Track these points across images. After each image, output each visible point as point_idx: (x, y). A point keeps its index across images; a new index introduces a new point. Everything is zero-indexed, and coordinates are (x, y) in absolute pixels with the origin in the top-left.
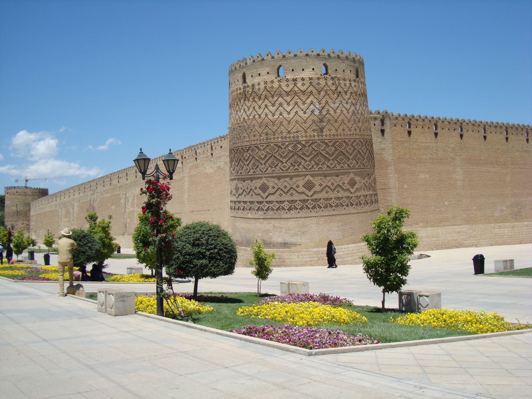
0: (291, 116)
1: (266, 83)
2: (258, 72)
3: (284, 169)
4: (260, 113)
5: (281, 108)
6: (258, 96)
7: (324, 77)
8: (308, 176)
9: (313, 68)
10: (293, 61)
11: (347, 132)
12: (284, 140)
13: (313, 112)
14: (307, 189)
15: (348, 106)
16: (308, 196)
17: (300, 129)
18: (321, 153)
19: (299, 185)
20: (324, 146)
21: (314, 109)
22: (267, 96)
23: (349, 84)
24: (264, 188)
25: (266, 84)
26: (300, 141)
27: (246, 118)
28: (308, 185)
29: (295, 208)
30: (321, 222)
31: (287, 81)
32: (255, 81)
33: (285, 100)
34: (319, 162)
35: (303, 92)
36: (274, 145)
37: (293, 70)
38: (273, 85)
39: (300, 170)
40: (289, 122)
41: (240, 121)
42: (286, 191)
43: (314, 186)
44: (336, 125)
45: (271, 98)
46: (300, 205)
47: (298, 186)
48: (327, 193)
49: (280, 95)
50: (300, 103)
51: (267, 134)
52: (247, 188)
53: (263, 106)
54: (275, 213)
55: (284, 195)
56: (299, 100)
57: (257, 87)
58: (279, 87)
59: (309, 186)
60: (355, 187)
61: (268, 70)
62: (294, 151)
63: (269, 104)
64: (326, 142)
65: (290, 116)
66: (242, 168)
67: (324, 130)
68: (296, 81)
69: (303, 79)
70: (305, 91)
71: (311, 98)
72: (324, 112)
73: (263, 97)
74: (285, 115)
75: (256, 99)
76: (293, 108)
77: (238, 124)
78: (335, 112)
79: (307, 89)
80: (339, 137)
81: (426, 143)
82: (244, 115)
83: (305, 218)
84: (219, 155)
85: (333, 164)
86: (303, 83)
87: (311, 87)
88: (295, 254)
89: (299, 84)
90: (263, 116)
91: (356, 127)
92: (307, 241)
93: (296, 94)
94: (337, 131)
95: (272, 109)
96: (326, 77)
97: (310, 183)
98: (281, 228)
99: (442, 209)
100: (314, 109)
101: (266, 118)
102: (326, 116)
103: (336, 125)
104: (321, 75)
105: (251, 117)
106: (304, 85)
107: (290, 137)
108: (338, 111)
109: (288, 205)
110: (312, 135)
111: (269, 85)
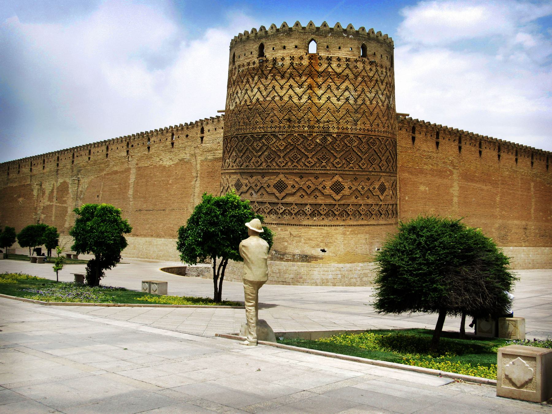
0: (322, 101)
1: (292, 58)
2: (283, 45)
3: (308, 165)
4: (281, 94)
6: (280, 73)
7: (362, 60)
8: (337, 176)
13: (347, 99)
14: (334, 192)
15: (383, 98)
16: (335, 200)
17: (332, 118)
18: (353, 150)
21: (349, 97)
22: (293, 75)
24: (281, 186)
25: (293, 60)
26: (331, 133)
27: (261, 99)
28: (336, 188)
29: (304, 213)
30: (348, 233)
31: (320, 60)
32: (278, 55)
33: (316, 82)
34: (350, 160)
35: (338, 75)
36: (298, 135)
37: (328, 47)
38: (302, 62)
39: (328, 168)
40: (319, 109)
41: (251, 102)
43: (343, 189)
44: (372, 118)
45: (298, 78)
46: (325, 210)
47: (324, 187)
48: (356, 199)
50: (333, 87)
51: (289, 120)
52: (256, 186)
53: (287, 86)
54: (293, 218)
55: (306, 197)
56: (333, 83)
58: (309, 65)
59: (337, 188)
61: (296, 42)
62: (323, 144)
63: (295, 85)
64: (359, 138)
65: (321, 101)
66: (250, 160)
67: (359, 123)
68: (331, 60)
69: (339, 59)
71: (347, 83)
72: (360, 102)
73: (287, 75)
75: (278, 78)
76: (325, 93)
77: (248, 106)
78: (371, 103)
79: (343, 72)
80: (373, 133)
81: (428, 152)
82: (258, 95)
83: (330, 227)
84: (183, 146)
85: (365, 164)
86: (339, 64)
88: (315, 269)
90: (286, 98)
92: (330, 254)
94: (371, 125)
95: (299, 91)
96: (364, 61)
97: (339, 185)
98: (300, 237)
100: (349, 97)
101: (290, 101)
103: (372, 118)
104: (359, 57)
106: (340, 66)
108: (374, 102)
109: (311, 210)
111: (296, 62)
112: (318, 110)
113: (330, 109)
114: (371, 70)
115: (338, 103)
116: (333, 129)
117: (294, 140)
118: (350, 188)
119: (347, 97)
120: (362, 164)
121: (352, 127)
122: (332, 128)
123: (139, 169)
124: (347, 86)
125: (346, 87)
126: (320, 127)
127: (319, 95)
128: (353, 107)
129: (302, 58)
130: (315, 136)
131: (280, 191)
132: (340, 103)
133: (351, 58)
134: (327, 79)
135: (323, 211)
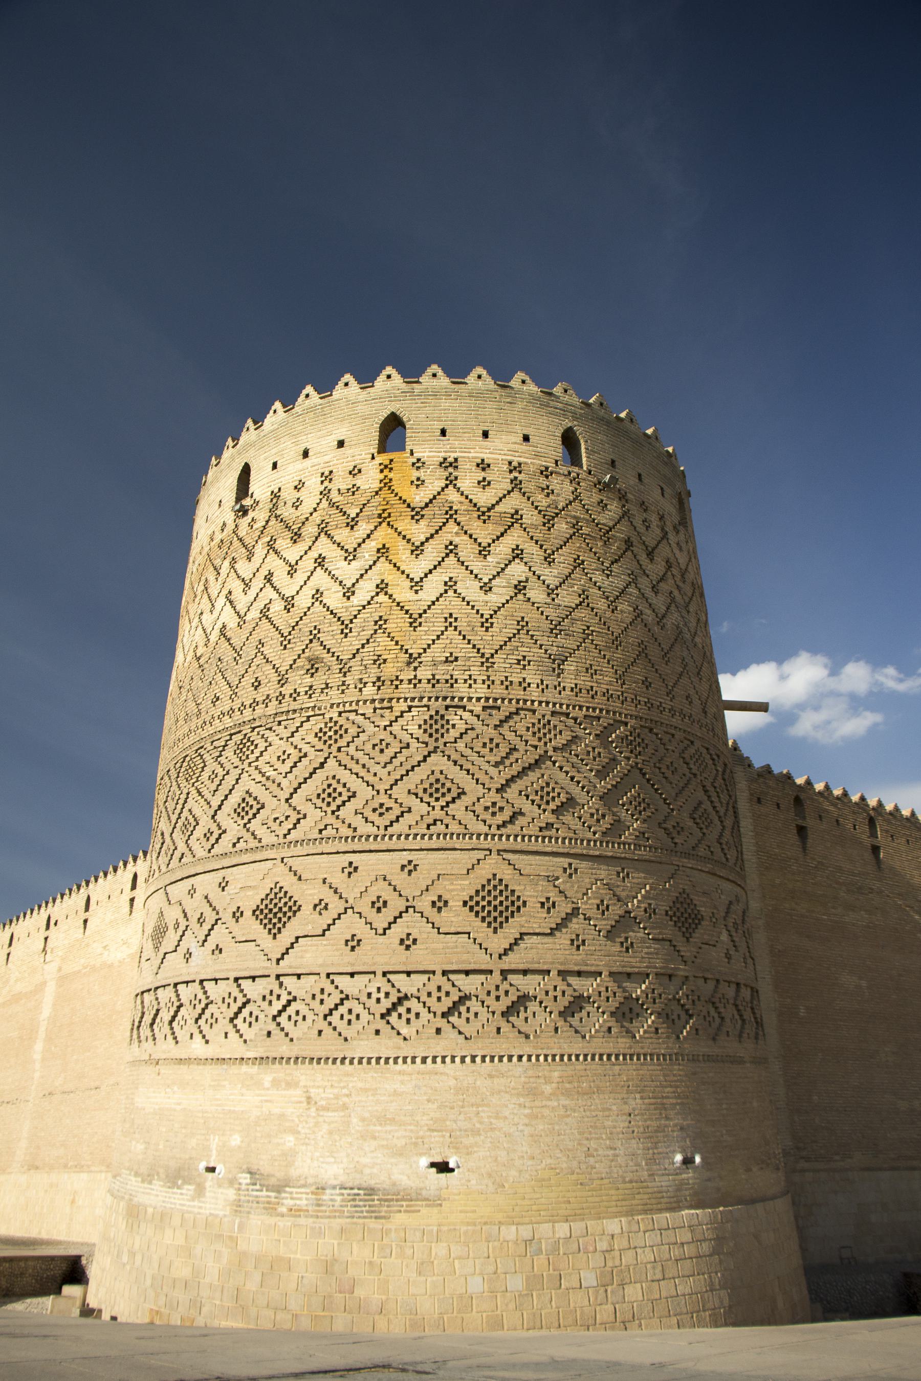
1: (327, 477)
5: (383, 565)
7: (569, 473)
9: (526, 432)
10: (445, 403)
12: (387, 691)
19: (444, 898)
20: (567, 736)
21: (527, 581)
26: (461, 699)
30: (548, 1089)
31: (418, 468)
35: (484, 514)
37: (443, 432)
39: (454, 828)
42: (380, 921)
43: (519, 908)
47: (440, 904)
49: (384, 518)
50: (467, 550)
51: (312, 670)
53: (308, 563)
54: (320, 1032)
57: (288, 495)
58: (381, 489)
69: (483, 466)
70: (489, 510)
71: (515, 537)
73: (310, 530)
74: (402, 592)
75: (281, 544)
79: (498, 503)
85: (604, 816)
86: (484, 479)
87: (516, 494)
89: (468, 481)
90: (303, 601)
91: (692, 692)
93: (451, 514)
95: (348, 571)
98: (345, 1107)
100: (527, 581)
102: (576, 614)
105: (254, 614)
107: (415, 682)
110: (516, 679)
111: (342, 482)
112: (411, 623)
113: (456, 619)
116: (470, 686)
117: (325, 733)
118: (547, 905)
119: (520, 582)
121: (542, 681)
122: (466, 681)
123: (63, 979)
124: (518, 546)
125: (513, 550)
126: (420, 681)
127: (417, 575)
129: (360, 471)
130: (402, 712)
131: (275, 931)
132: (491, 597)
133: (525, 463)
134: (444, 524)
135: (439, 999)
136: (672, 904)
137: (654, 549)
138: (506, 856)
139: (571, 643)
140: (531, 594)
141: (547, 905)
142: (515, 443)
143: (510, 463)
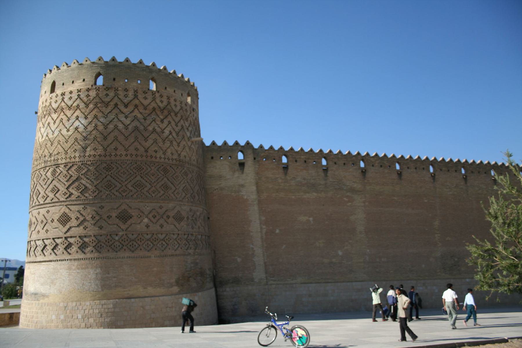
9: (84, 78)
11: (121, 151)
14: (61, 224)
15: (127, 122)
20: (86, 170)
21: (79, 126)
23: (132, 95)
30: (74, 268)
35: (70, 108)
43: (70, 220)
44: (106, 143)
60: (129, 222)
67: (88, 149)
71: (78, 113)
93: (62, 109)
94: (105, 150)
97: (66, 216)
99: (334, 260)
107: (51, 161)
108: (111, 127)
110: (72, 156)
114: (107, 95)
115: (67, 133)
118: (77, 218)
120: (92, 192)
128: (82, 135)
133: (82, 89)
136: (118, 214)
137: (128, 104)
138: (68, 206)
139: (89, 142)
140: (79, 130)
141: (77, 218)
142: (80, 83)
143: (78, 90)
